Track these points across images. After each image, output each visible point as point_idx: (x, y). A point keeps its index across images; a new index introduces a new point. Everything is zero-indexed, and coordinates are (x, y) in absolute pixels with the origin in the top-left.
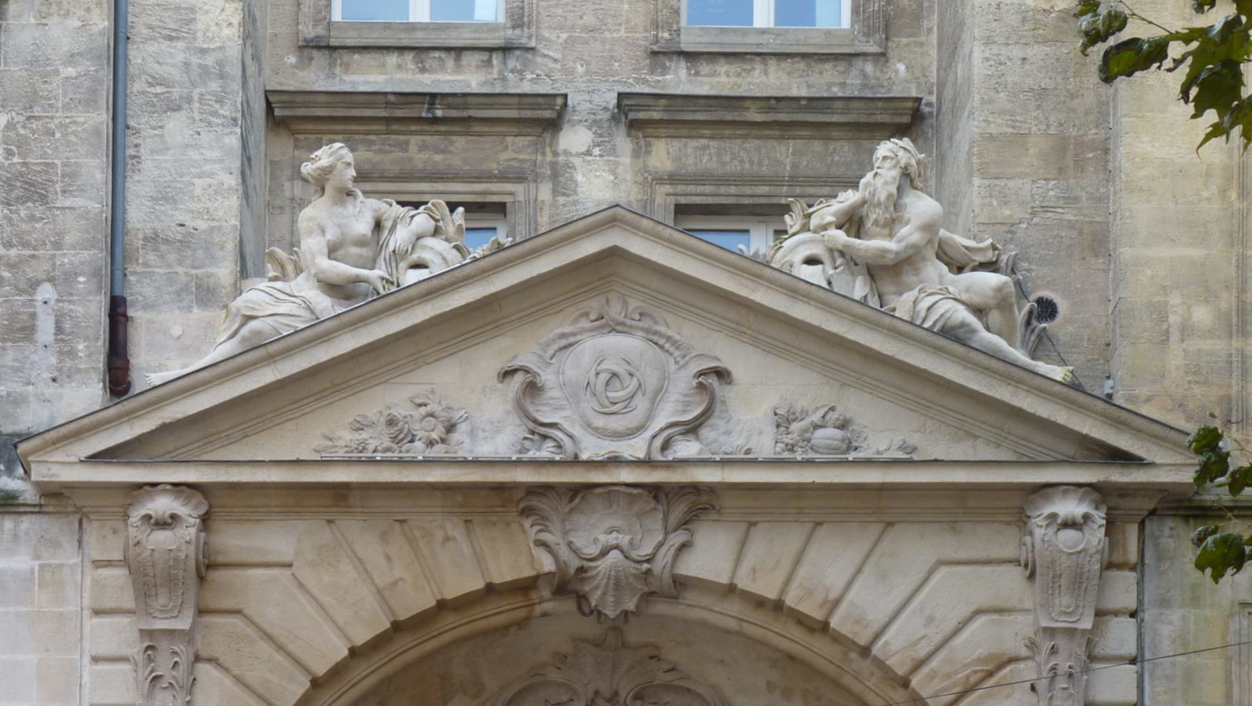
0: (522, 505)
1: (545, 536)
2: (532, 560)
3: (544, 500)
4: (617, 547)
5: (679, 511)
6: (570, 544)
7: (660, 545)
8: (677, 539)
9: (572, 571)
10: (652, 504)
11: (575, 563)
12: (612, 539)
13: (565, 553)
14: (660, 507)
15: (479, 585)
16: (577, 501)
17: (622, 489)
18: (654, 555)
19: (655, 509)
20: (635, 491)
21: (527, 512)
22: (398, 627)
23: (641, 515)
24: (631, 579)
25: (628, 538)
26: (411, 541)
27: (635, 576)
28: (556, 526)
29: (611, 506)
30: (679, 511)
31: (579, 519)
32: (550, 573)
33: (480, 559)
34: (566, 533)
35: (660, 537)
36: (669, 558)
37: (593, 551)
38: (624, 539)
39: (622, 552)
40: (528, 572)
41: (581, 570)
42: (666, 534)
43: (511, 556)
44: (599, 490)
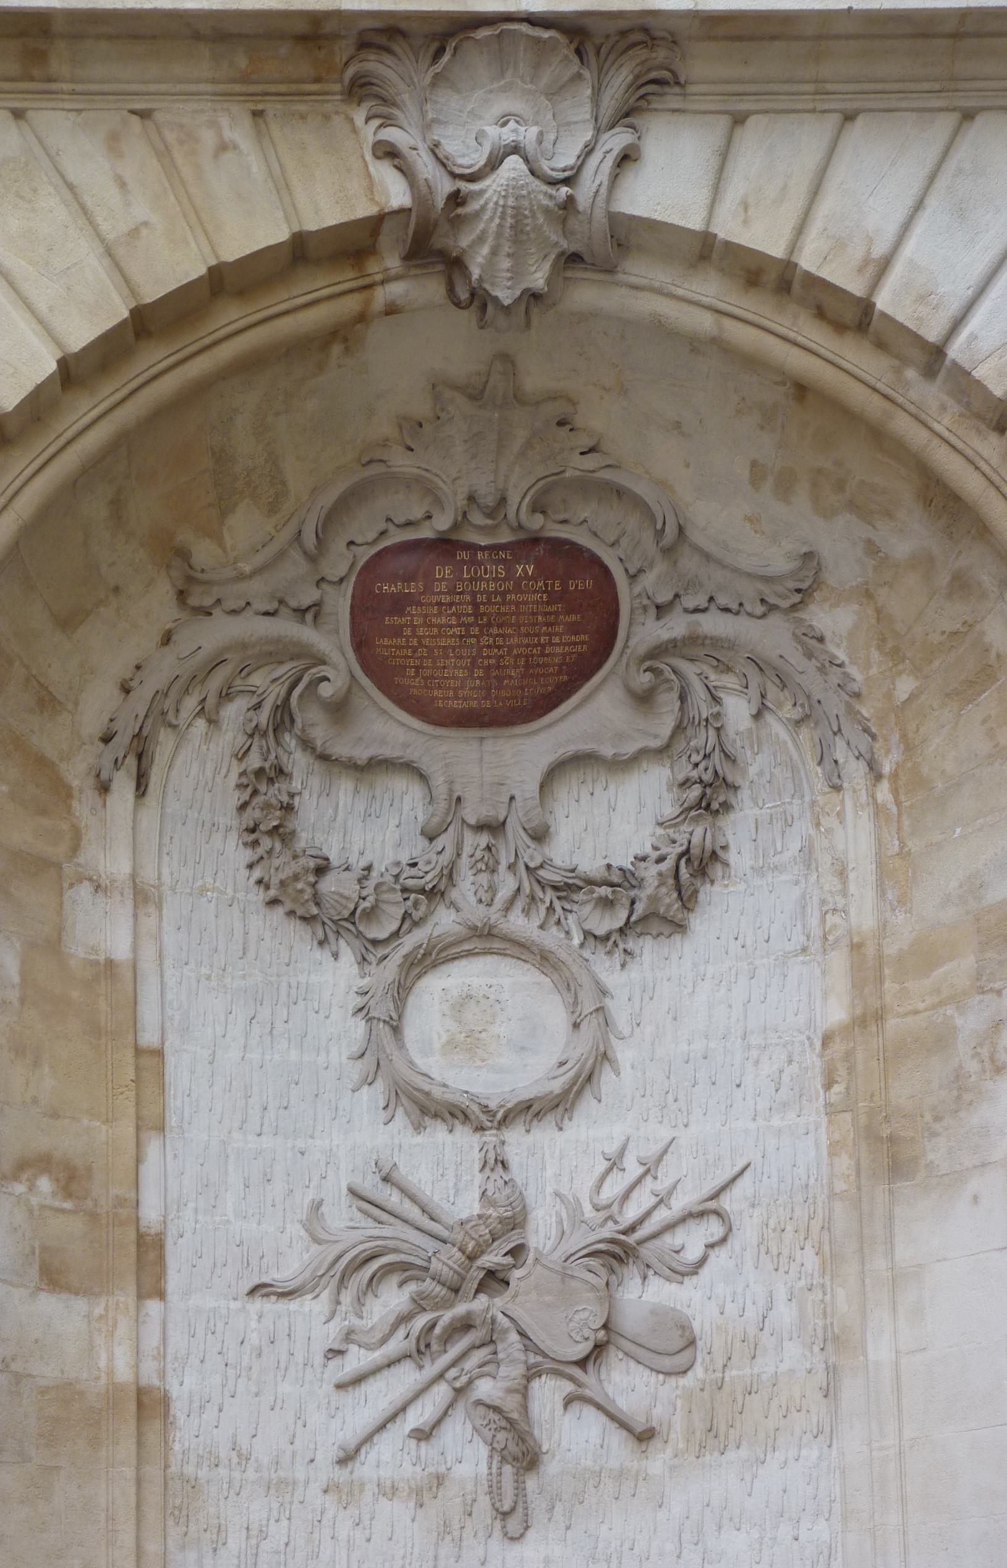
0: (350, 72)
1: (391, 134)
2: (371, 185)
3: (388, 59)
4: (515, 149)
5: (620, 79)
6: (434, 148)
7: (588, 151)
8: (617, 140)
9: (440, 203)
10: (575, 66)
11: (445, 186)
12: (508, 134)
13: (426, 167)
14: (586, 73)
15: (281, 235)
16: (446, 58)
17: (524, 28)
18: (579, 168)
19: (578, 76)
20: (546, 34)
21: (360, 89)
22: (145, 324)
23: (554, 93)
24: (541, 220)
25: (534, 131)
26: (164, 154)
27: (547, 211)
28: (409, 113)
29: (502, 75)
30: (620, 79)
31: (448, 101)
32: (401, 211)
33: (282, 186)
34: (427, 127)
35: (588, 135)
36: (604, 177)
37: (476, 159)
38: (528, 135)
39: (526, 160)
40: (364, 210)
41: (456, 199)
42: (598, 131)
43: (336, 179)
44: (483, 33)
